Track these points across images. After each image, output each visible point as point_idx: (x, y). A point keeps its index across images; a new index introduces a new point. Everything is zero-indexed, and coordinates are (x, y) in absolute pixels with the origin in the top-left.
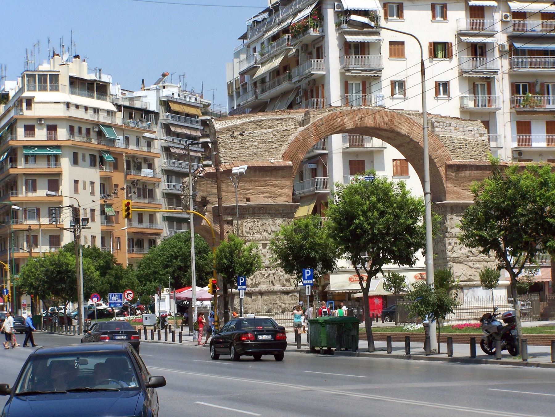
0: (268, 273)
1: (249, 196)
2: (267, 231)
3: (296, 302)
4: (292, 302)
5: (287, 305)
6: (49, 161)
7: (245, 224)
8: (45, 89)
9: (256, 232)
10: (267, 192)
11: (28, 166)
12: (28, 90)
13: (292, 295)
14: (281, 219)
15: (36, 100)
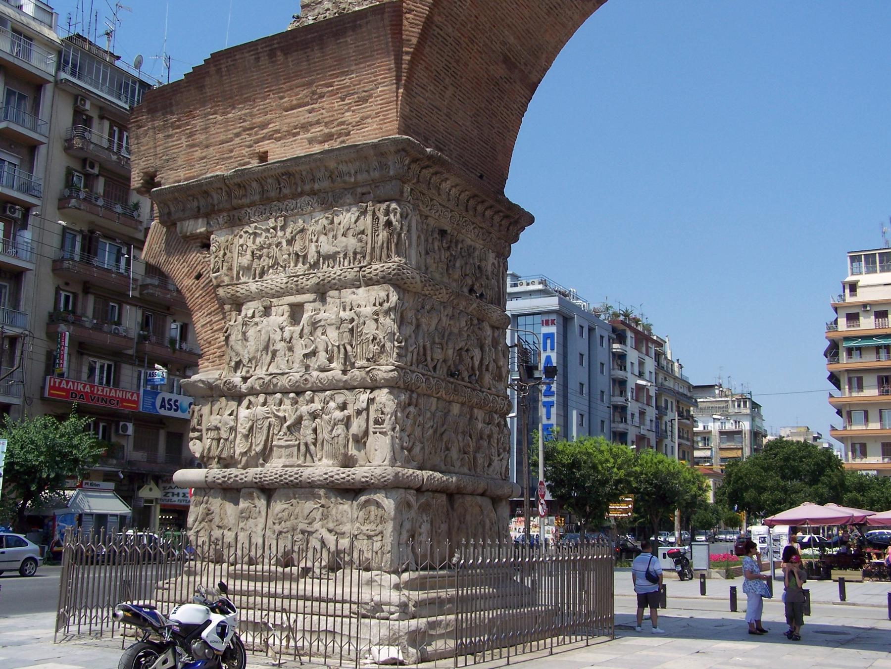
0: (298, 413)
1: (265, 146)
2: (305, 257)
3: (380, 528)
4: (364, 528)
5: (344, 543)
6: (878, 353)
7: (241, 241)
8: (875, 272)
9: (272, 267)
10: (318, 122)
11: (850, 361)
12: (852, 274)
13: (367, 502)
14: (354, 209)
15: (860, 284)
